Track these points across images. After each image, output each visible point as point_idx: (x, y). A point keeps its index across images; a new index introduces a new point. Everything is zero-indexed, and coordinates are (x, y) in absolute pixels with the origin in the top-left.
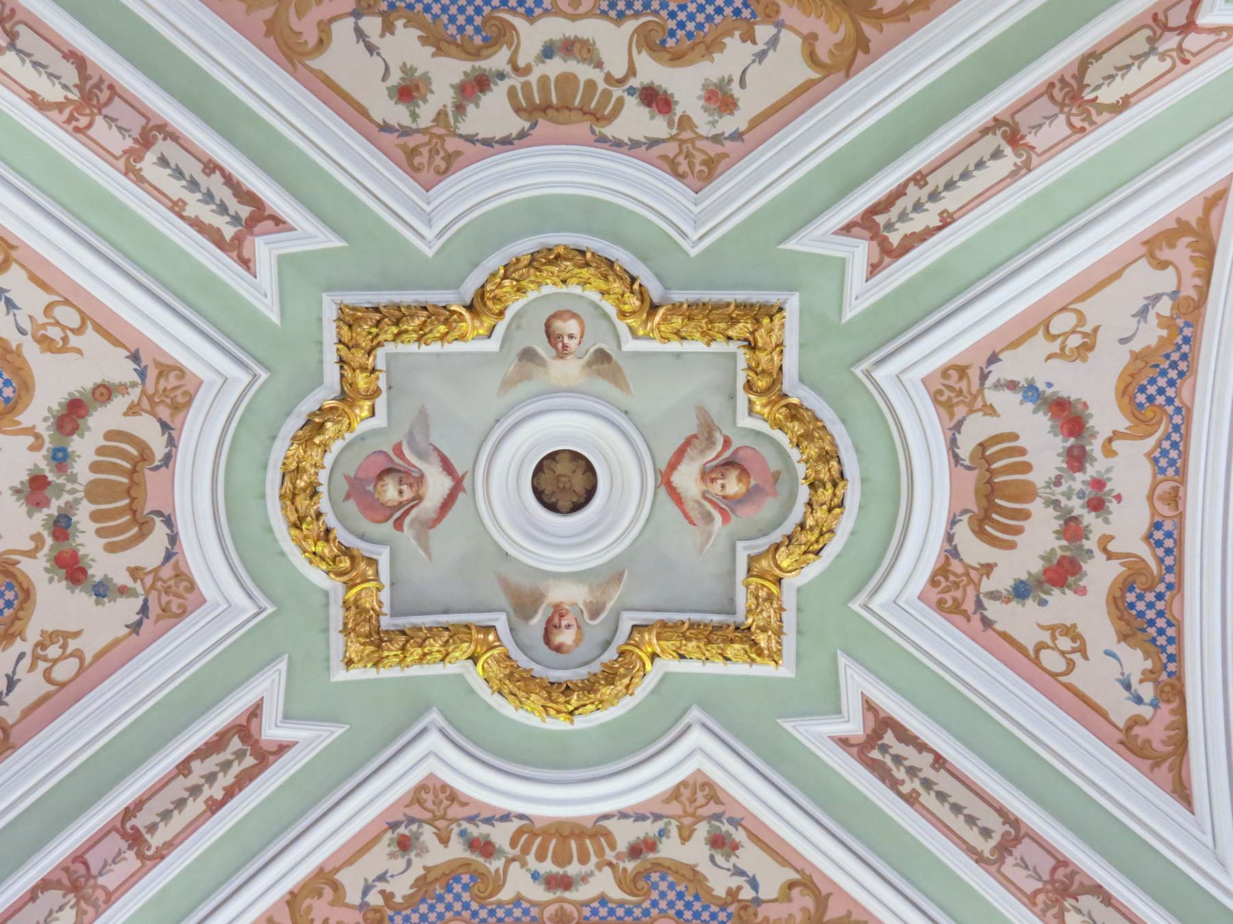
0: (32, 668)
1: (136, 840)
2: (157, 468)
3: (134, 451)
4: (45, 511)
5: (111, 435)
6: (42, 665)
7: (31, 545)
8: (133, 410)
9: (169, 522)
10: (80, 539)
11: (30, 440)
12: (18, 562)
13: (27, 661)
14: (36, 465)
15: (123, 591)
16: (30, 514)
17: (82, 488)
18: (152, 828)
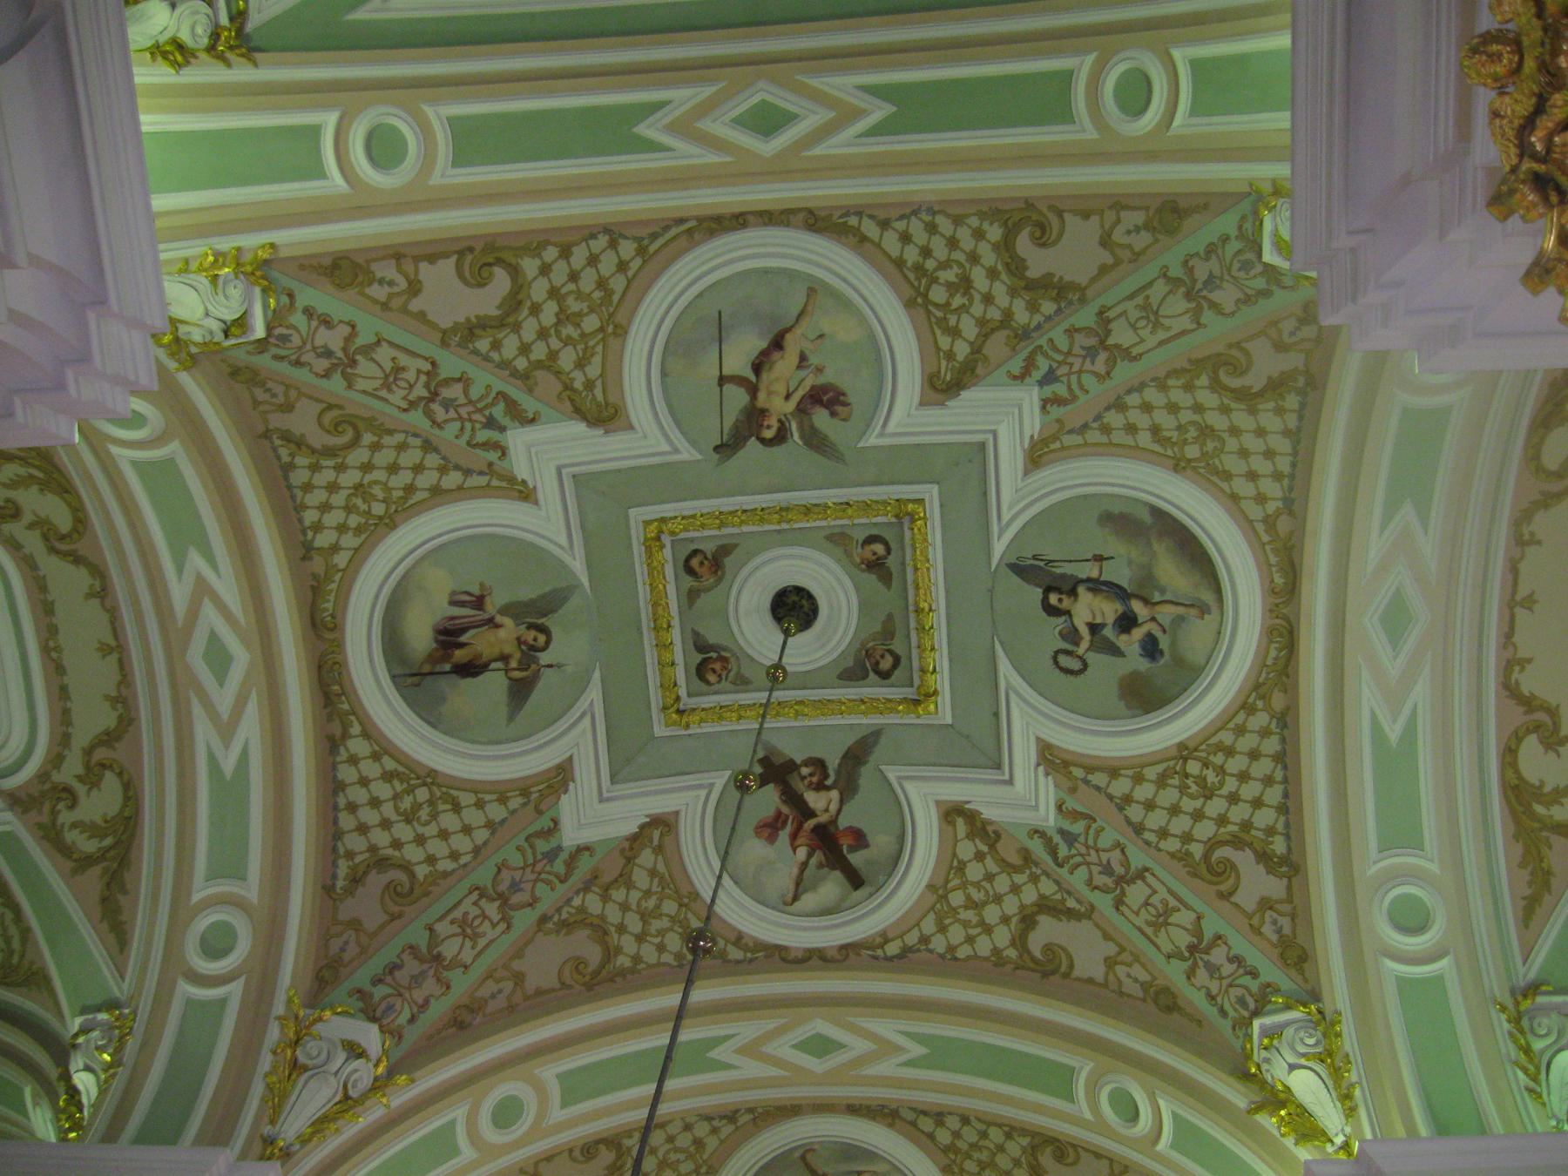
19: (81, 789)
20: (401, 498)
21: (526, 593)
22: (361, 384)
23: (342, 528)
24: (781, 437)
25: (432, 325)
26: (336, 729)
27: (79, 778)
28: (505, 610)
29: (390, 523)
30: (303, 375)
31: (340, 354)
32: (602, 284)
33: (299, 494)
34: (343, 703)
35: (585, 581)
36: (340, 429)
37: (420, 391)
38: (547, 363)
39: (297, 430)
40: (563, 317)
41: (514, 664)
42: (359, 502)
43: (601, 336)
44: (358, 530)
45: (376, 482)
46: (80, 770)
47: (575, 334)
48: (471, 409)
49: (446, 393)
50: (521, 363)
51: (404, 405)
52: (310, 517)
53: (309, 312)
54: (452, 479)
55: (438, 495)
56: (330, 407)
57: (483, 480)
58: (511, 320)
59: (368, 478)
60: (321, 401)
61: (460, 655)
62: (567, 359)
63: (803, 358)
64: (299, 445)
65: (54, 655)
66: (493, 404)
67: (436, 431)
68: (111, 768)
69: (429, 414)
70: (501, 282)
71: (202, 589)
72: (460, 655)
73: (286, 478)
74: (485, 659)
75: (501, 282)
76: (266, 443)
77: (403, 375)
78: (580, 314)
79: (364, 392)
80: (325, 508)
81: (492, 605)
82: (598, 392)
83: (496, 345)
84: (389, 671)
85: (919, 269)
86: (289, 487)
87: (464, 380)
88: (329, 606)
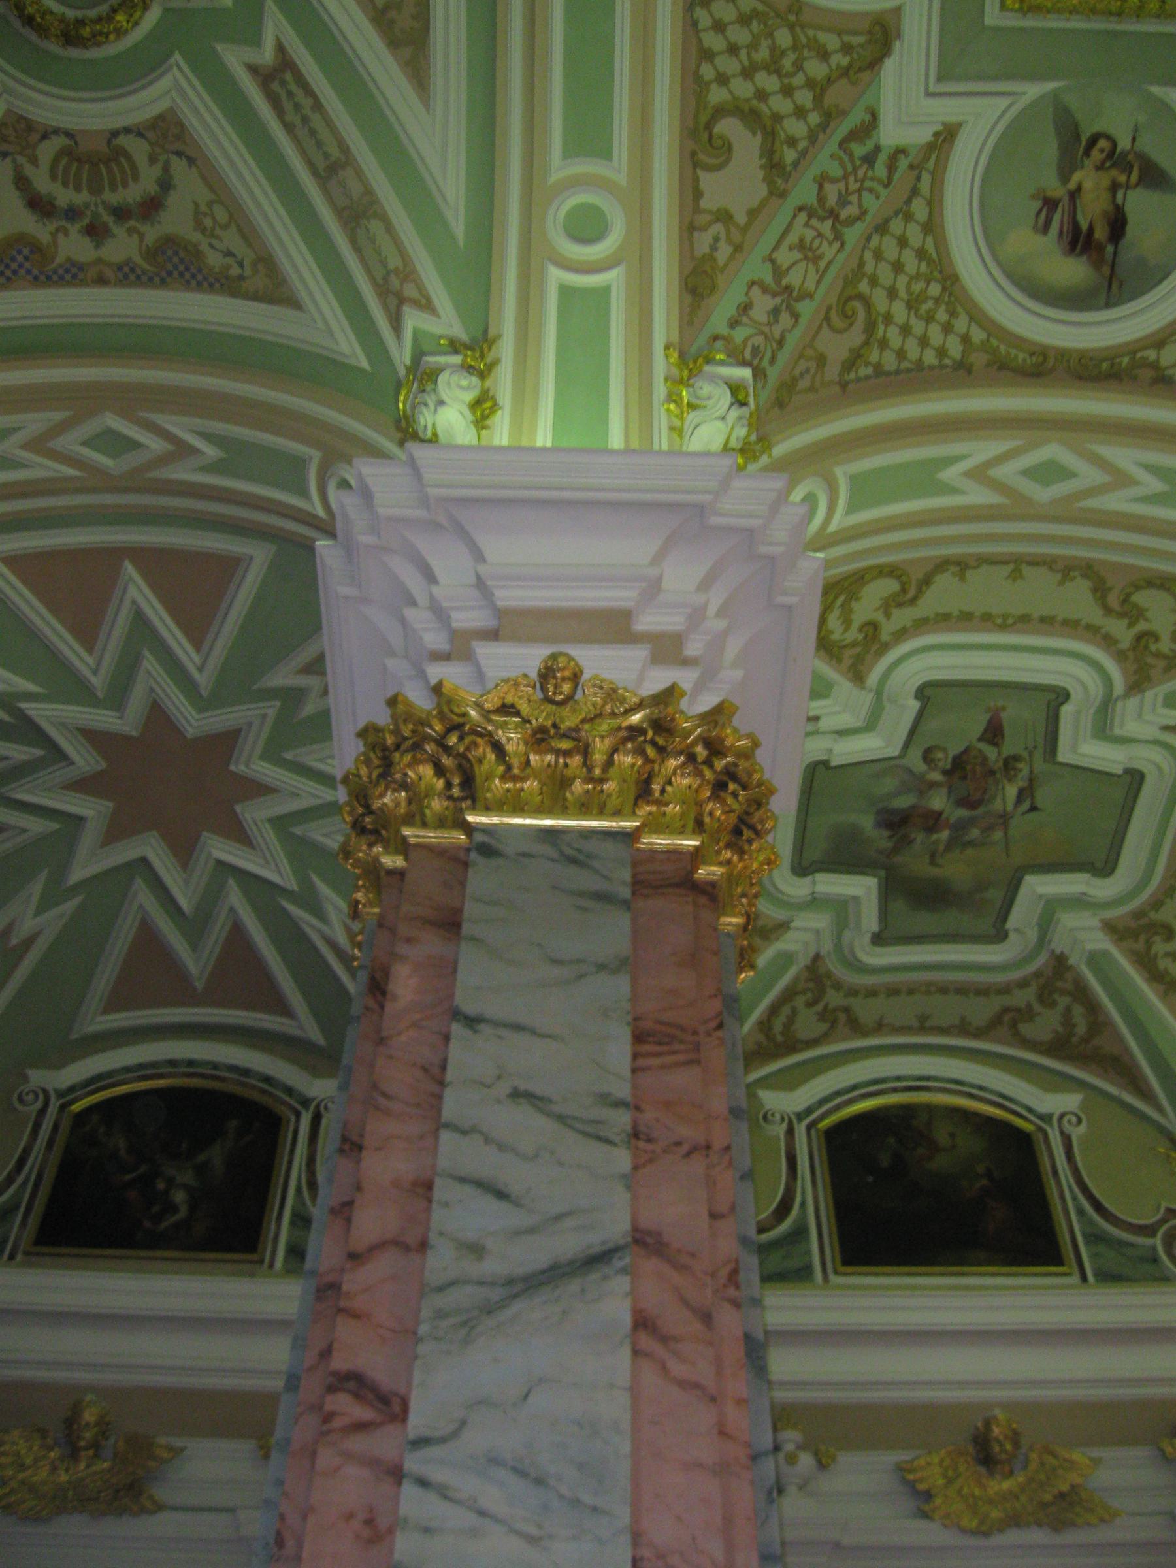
0: (219, 238)
1: (333, 168)
2: (76, 143)
3: (64, 161)
4: (111, 224)
5: (53, 177)
6: (218, 231)
7: (135, 236)
8: (34, 161)
9: (115, 134)
10: (130, 200)
11: (61, 236)
12: (148, 246)
13: (215, 242)
14: (79, 232)
15: (166, 168)
16: (113, 236)
17: (94, 198)
18: (326, 156)
19: (1142, 626)
20: (928, 264)
21: (1050, 151)
22: (810, 285)
23: (947, 329)
25: (763, 205)
26: (1147, 374)
27: (1131, 625)
28: (1065, 177)
29: (950, 280)
31: (778, 300)
33: (905, 365)
34: (1120, 364)
35: (1050, 86)
36: (850, 313)
37: (826, 227)
38: (818, 90)
39: (844, 354)
40: (773, 67)
41: (1122, 179)
42: (924, 308)
43: (798, 29)
44: (953, 314)
45: (908, 287)
46: (1125, 622)
47: (792, 56)
48: (852, 179)
49: (832, 201)
50: (814, 118)
51: (837, 245)
52: (930, 358)
53: (734, 324)
54: (919, 209)
55: (932, 226)
57: (926, 178)
58: (768, 123)
59: (902, 293)
60: (820, 327)
61: (1100, 234)
62: (816, 69)
64: (859, 356)
65: (1010, 621)
66: (851, 155)
67: (868, 218)
68: (1128, 595)
69: (851, 221)
70: (728, 127)
71: (979, 474)
72: (1100, 234)
73: (889, 374)
74: (1110, 208)
75: (728, 127)
76: (851, 387)
77: (808, 241)
78: (773, 49)
79: (818, 282)
80: (924, 342)
81: (1057, 190)
83: (792, 142)
84: (1098, 309)
86: (898, 372)
87: (822, 181)
88: (1021, 356)
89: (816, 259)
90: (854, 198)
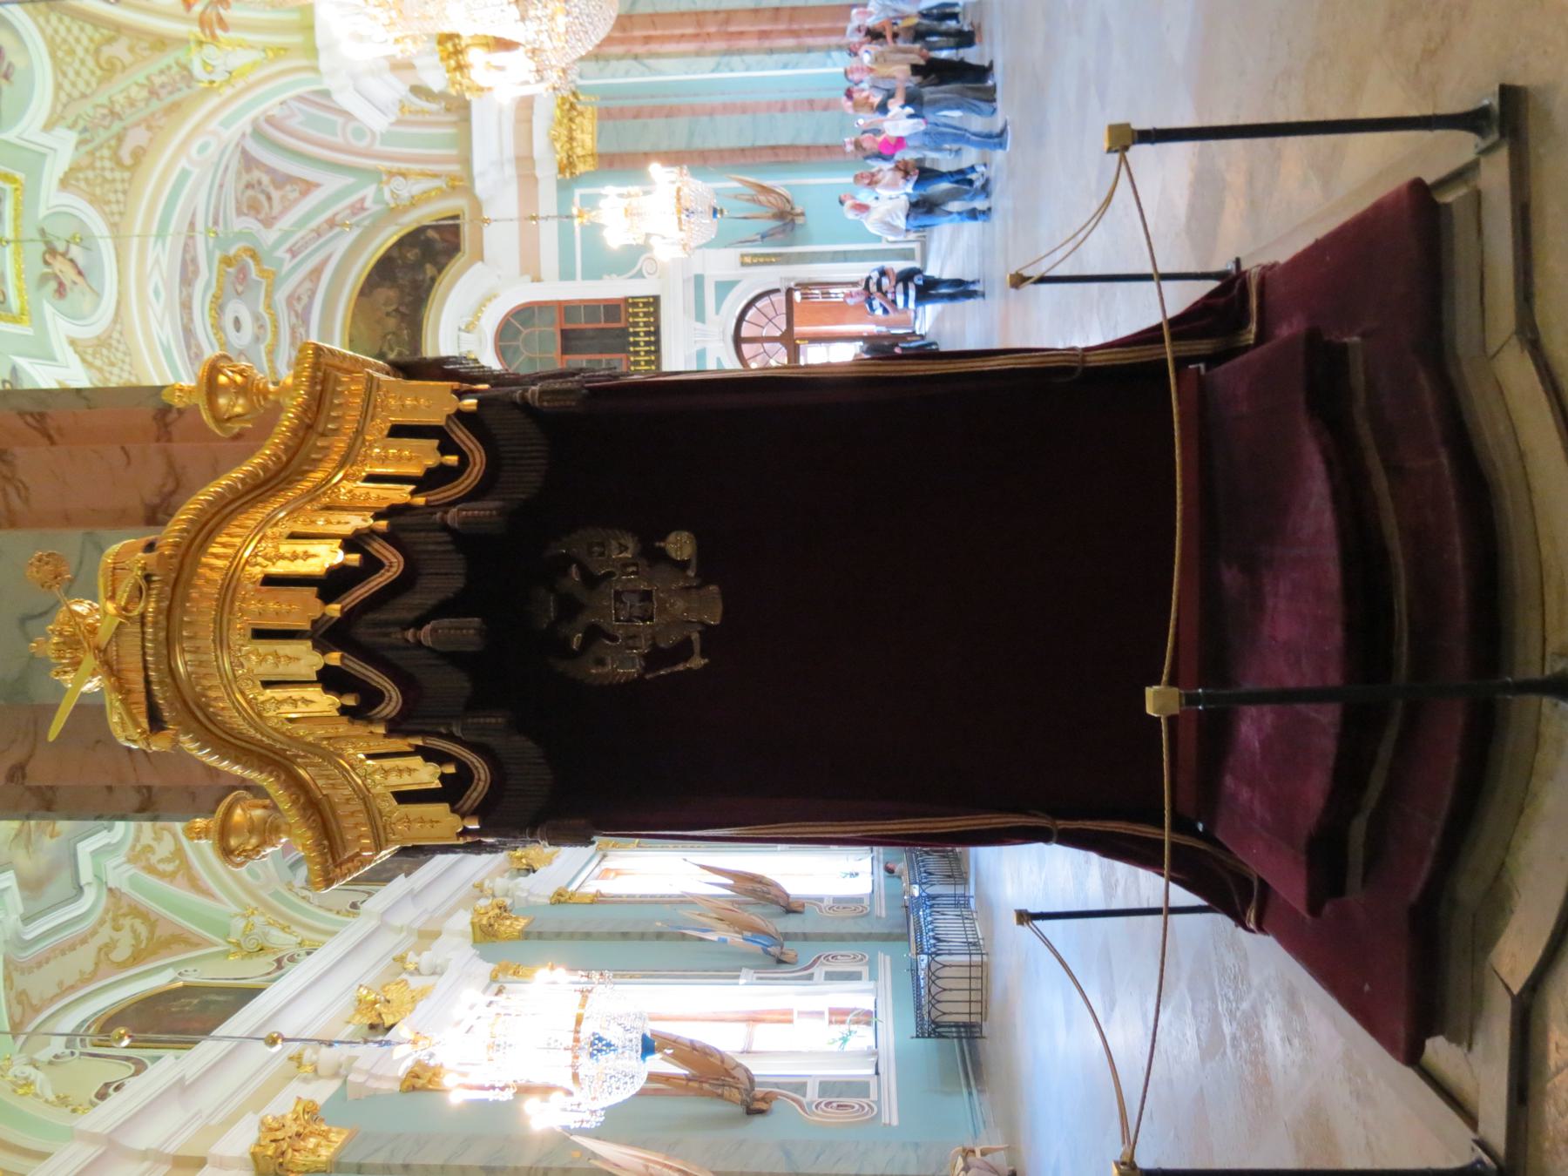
23: (56, 31)
24: (46, 263)
29: (53, 55)
30: (153, 69)
32: (108, 202)
37: (118, 108)
40: (105, 180)
42: (65, 47)
44: (52, 38)
49: (109, 119)
50: (98, 154)
52: (67, 20)
54: (63, 97)
55: (59, 87)
56: (124, 68)
59: (77, 61)
62: (90, 174)
63: (75, 283)
69: (102, 106)
70: (128, 161)
75: (128, 161)
80: (69, 30)
82: (73, 182)
83: (110, 147)
85: (110, 345)
86: (85, 21)
89: (128, 98)
90: (98, 115)
